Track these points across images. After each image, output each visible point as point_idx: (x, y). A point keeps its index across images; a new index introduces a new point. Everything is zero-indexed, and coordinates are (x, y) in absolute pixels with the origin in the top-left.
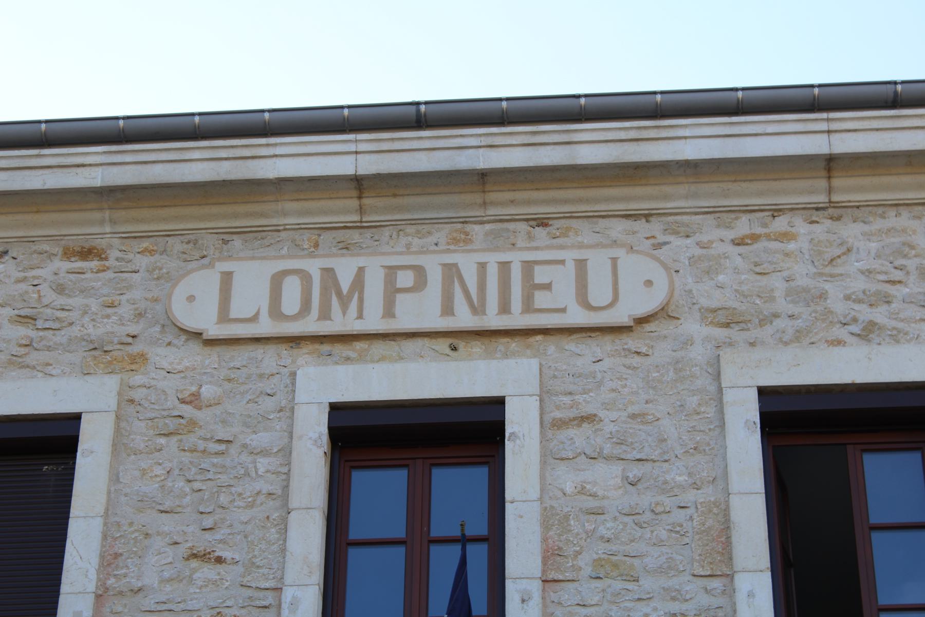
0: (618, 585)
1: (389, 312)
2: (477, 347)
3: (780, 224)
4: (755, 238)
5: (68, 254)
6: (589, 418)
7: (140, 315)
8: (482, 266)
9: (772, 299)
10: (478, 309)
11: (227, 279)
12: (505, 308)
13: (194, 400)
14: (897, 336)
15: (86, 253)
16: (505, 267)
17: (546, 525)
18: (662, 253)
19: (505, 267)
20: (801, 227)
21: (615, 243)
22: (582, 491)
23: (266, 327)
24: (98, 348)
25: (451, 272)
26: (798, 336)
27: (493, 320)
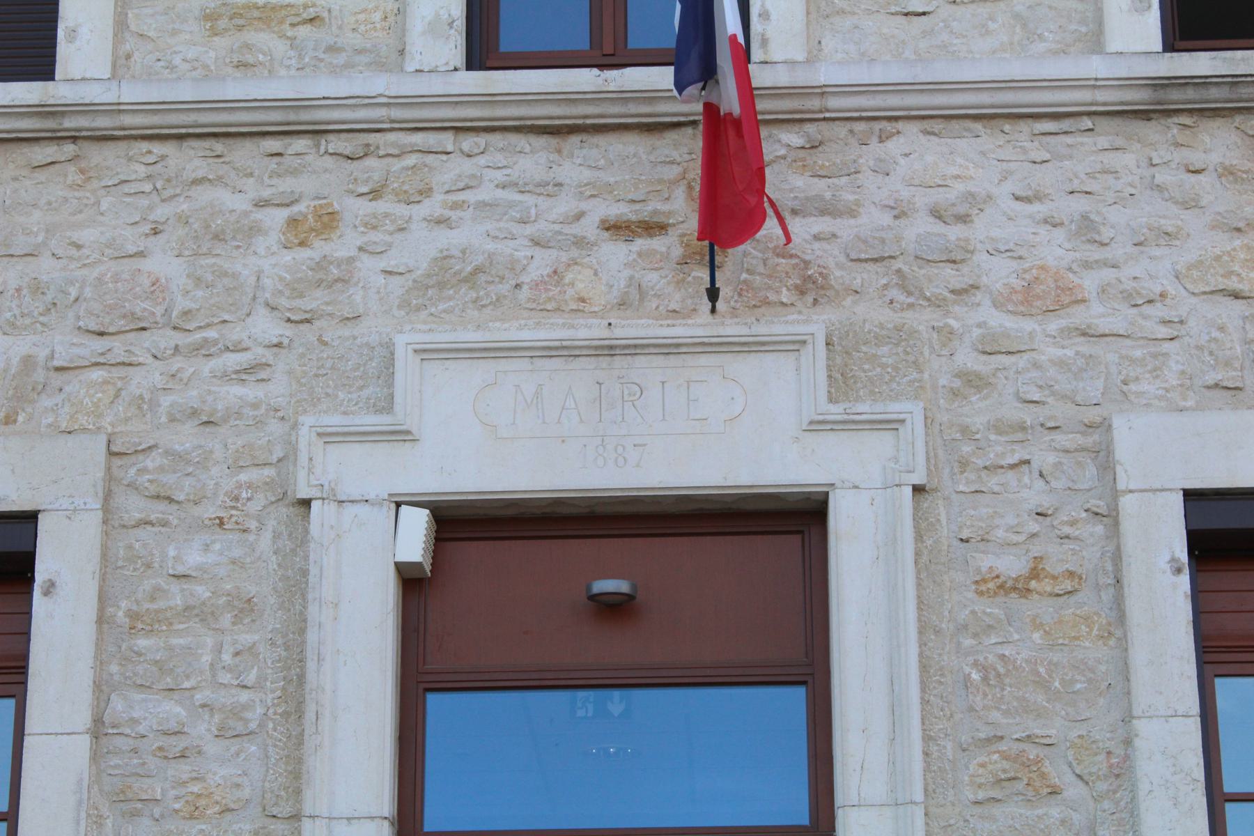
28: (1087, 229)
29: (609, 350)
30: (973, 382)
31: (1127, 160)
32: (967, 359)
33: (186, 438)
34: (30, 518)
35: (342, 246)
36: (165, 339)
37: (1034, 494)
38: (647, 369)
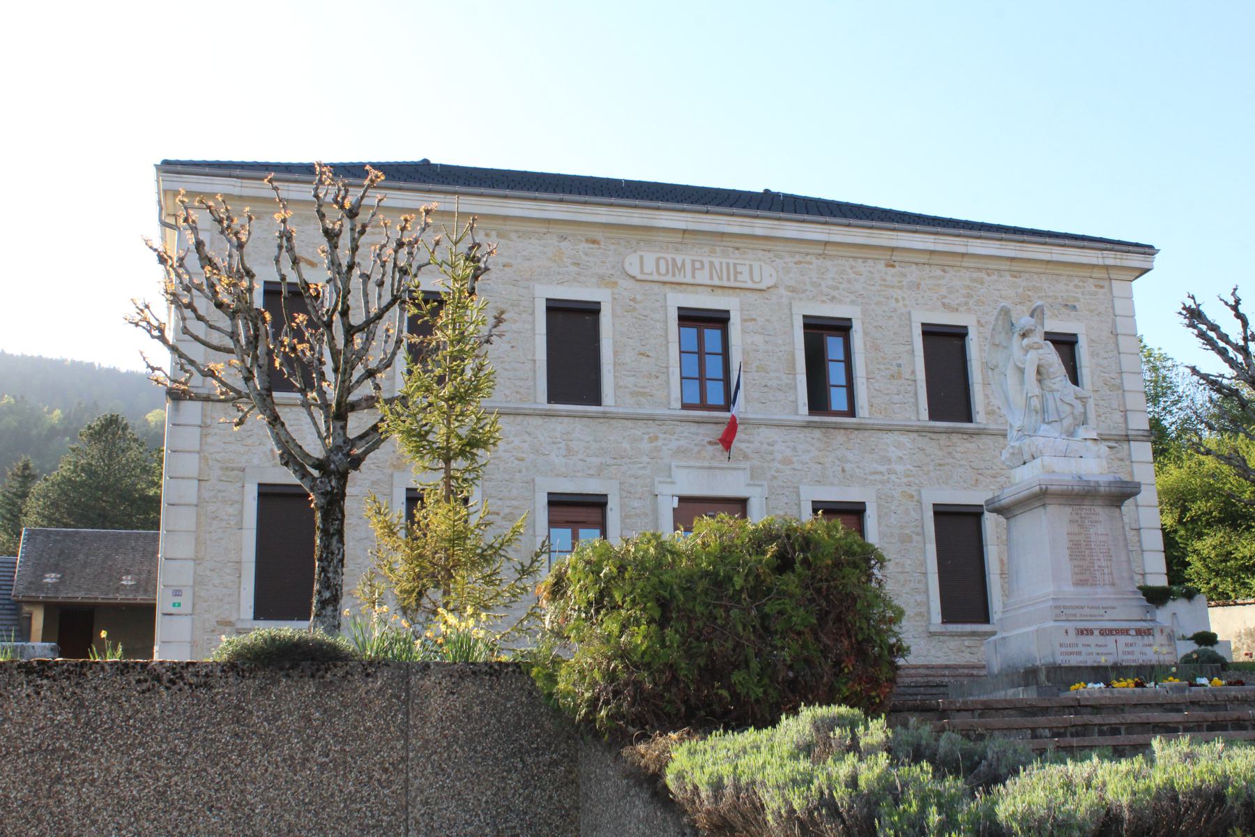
0: (764, 374)
1: (693, 277)
2: (719, 291)
3: (808, 258)
4: (801, 262)
5: (587, 241)
6: (754, 320)
7: (614, 267)
8: (721, 263)
9: (805, 285)
10: (720, 278)
11: (642, 257)
12: (729, 279)
13: (634, 300)
14: (841, 302)
15: (594, 242)
16: (728, 264)
17: (743, 353)
18: (774, 264)
19: (728, 264)
20: (814, 260)
21: (760, 260)
22: (752, 343)
23: (655, 277)
24: (601, 277)
25: (712, 264)
26: (813, 298)
27: (726, 283)
28: (794, 449)
29: (711, 468)
30: (775, 477)
31: (801, 436)
32: (773, 473)
33: (632, 481)
34: (606, 496)
35: (659, 443)
36: (628, 461)
37: (785, 500)
38: (717, 471)
